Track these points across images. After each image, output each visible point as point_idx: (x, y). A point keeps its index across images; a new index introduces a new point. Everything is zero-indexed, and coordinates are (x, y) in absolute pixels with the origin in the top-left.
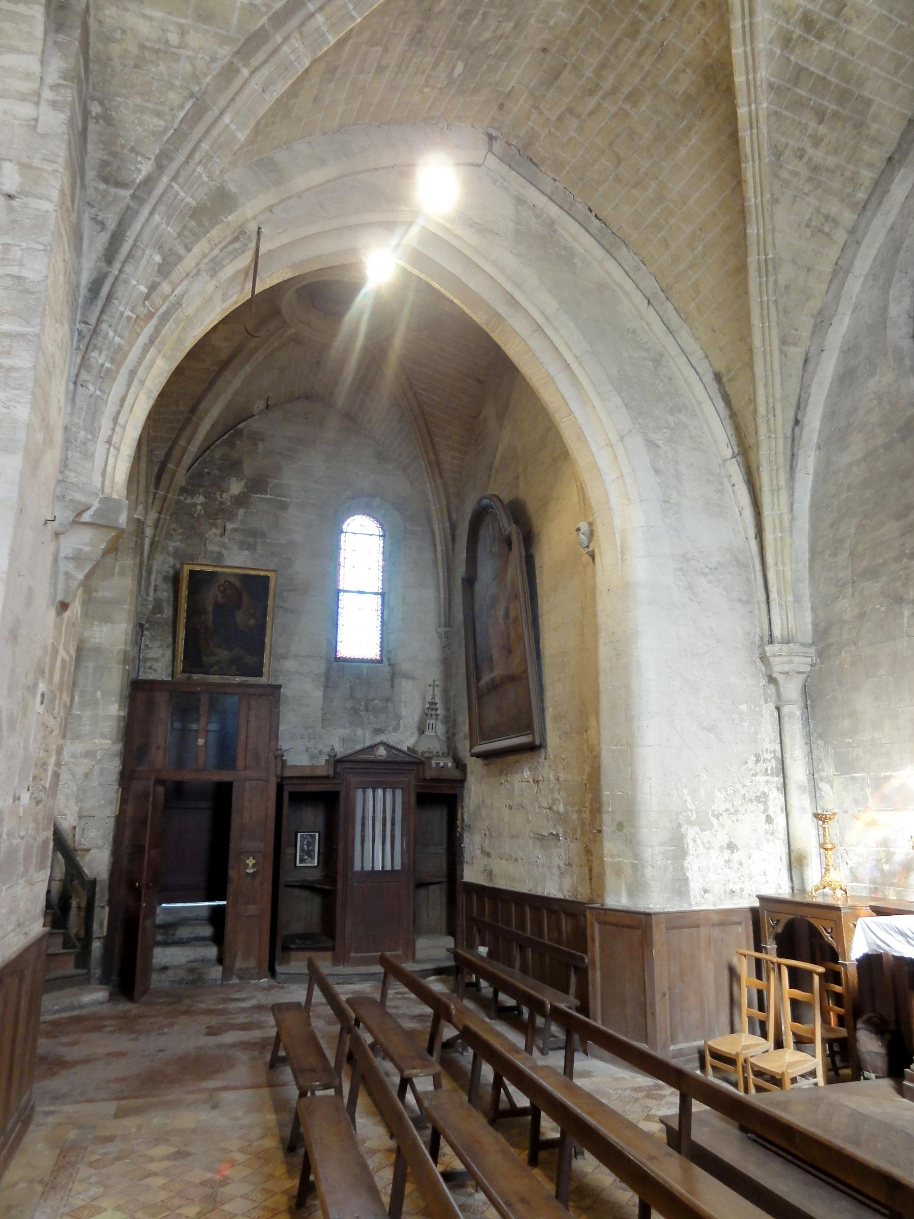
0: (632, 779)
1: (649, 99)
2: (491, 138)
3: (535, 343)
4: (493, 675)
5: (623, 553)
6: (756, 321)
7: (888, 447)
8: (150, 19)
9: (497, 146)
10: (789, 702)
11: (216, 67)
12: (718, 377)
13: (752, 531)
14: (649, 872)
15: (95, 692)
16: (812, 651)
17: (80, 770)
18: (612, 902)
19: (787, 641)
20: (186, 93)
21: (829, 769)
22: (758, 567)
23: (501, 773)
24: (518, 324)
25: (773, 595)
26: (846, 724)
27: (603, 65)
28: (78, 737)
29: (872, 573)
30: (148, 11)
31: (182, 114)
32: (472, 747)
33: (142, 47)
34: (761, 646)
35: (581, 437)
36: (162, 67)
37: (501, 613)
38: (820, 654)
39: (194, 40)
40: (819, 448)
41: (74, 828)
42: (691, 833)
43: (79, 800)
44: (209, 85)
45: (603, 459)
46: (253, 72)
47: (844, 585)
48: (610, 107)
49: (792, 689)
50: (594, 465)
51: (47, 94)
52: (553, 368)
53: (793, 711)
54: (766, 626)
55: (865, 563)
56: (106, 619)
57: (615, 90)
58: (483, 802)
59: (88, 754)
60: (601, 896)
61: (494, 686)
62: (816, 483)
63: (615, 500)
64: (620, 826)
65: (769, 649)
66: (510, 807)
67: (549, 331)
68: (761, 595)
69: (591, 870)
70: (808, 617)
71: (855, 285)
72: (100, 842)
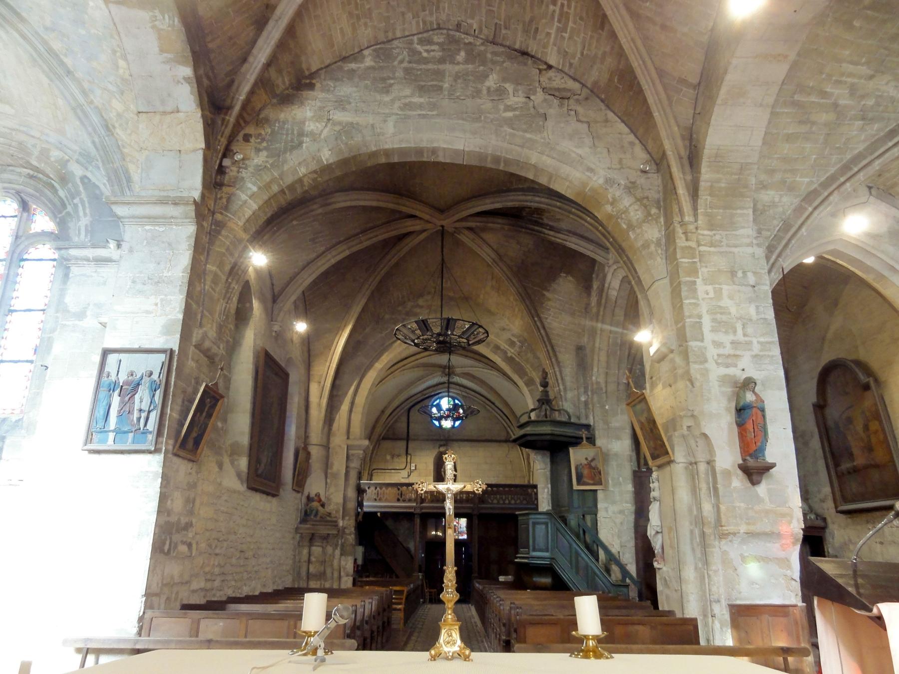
2: (870, 188)
4: (855, 464)
8: (768, 195)
9: (873, 191)
11: (793, 207)
15: (619, 478)
17: (618, 521)
20: (780, 220)
23: (868, 522)
28: (614, 503)
30: (768, 192)
31: (778, 228)
32: (836, 507)
33: (764, 206)
36: (771, 211)
37: (859, 428)
39: (785, 199)
41: (619, 552)
43: (619, 537)
44: (790, 215)
46: (815, 208)
51: (755, 242)
56: (618, 438)
58: (850, 541)
59: (621, 512)
61: (855, 470)
66: (881, 543)
72: (631, 560)
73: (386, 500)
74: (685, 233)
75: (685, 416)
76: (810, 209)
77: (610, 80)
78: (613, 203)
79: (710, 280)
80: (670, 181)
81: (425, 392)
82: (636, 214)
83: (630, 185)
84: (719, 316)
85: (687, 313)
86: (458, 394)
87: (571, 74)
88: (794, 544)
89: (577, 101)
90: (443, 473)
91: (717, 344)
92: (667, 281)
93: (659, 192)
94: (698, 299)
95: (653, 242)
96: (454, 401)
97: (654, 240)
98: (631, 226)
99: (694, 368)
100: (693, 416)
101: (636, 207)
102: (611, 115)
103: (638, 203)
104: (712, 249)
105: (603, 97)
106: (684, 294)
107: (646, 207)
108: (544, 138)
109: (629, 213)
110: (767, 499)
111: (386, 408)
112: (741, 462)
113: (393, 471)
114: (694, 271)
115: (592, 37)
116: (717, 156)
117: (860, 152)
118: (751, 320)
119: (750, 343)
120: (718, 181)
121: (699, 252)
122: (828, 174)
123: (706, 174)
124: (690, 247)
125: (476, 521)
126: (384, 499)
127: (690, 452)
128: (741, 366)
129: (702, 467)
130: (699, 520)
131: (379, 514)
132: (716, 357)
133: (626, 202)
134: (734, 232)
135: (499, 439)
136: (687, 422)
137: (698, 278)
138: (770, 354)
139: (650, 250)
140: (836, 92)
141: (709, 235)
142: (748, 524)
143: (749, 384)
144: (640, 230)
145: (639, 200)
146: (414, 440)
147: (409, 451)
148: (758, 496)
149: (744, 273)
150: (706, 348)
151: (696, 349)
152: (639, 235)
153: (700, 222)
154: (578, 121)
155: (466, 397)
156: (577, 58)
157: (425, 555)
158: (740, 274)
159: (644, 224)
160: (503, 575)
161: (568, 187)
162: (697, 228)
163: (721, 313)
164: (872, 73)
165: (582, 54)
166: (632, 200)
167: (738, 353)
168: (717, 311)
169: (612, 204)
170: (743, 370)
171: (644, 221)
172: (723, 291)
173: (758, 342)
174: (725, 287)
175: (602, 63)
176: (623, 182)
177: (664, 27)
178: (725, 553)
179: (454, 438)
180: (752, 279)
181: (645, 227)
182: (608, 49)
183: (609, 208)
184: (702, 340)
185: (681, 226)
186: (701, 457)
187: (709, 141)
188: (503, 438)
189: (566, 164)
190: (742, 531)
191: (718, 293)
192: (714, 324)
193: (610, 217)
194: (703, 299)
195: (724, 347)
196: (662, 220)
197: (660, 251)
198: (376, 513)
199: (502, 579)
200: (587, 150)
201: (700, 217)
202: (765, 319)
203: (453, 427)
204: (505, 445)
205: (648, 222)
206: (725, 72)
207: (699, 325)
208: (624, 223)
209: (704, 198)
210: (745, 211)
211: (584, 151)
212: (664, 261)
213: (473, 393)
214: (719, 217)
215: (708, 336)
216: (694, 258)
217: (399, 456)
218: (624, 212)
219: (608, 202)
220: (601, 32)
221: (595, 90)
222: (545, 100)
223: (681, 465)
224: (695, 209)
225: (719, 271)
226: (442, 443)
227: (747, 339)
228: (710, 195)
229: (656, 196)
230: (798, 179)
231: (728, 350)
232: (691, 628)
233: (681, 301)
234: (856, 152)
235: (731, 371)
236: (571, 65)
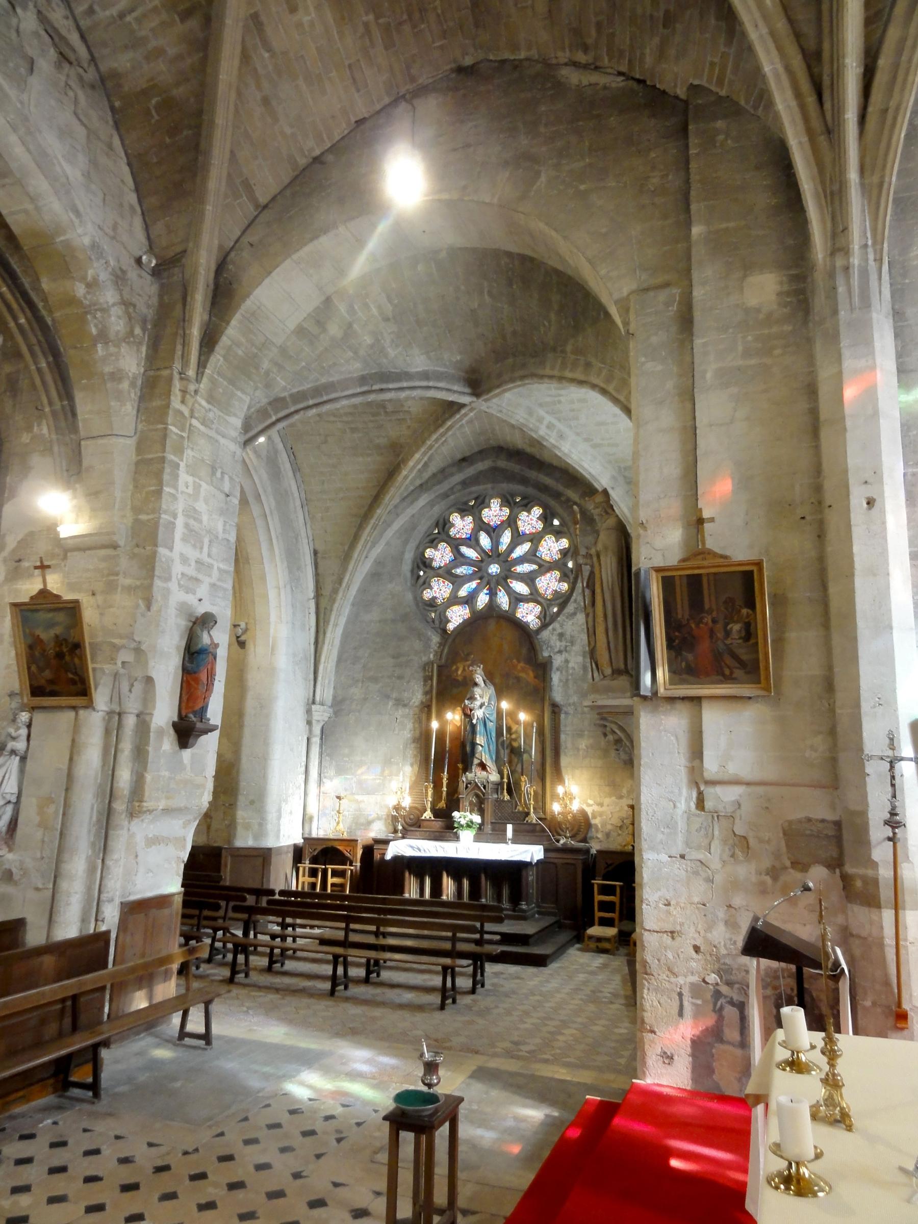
0: (263, 777)
1: (360, 435)
3: (259, 522)
5: (273, 649)
6: (359, 546)
7: (394, 621)
10: (315, 736)
11: (258, 406)
12: (316, 553)
13: (313, 640)
14: (269, 827)
16: (331, 710)
18: (239, 843)
19: (322, 704)
21: (332, 772)
22: (312, 661)
24: (255, 510)
25: (320, 678)
26: (346, 751)
27: (351, 414)
29: (374, 680)
34: (308, 704)
35: (263, 578)
38: (336, 713)
40: (353, 605)
42: (283, 805)
45: (272, 594)
46: (279, 420)
47: (358, 681)
48: (339, 425)
49: (317, 730)
50: (266, 596)
52: (262, 537)
53: (316, 740)
54: (312, 694)
55: (371, 673)
57: (347, 422)
60: (230, 840)
62: (347, 623)
63: (273, 617)
64: (252, 802)
65: (313, 707)
67: (269, 518)
68: (312, 676)
69: (209, 827)
70: (331, 692)
71: (390, 533)
74: (184, 392)
75: (124, 647)
76: (274, 418)
77: (145, 93)
78: (92, 285)
79: (192, 470)
80: (179, 306)
82: (117, 323)
83: (119, 273)
84: (192, 522)
85: (164, 506)
87: (82, 23)
88: (195, 819)
89: (81, 79)
91: (185, 560)
92: (131, 442)
93: (148, 307)
94: (177, 490)
95: (129, 377)
97: (130, 374)
98: (103, 336)
99: (158, 583)
100: (138, 651)
101: (120, 313)
102: (116, 141)
103: (123, 307)
104: (202, 428)
105: (117, 104)
106: (166, 477)
107: (130, 318)
108: (22, 103)
109: (110, 316)
110: (188, 768)
112: (176, 719)
114: (179, 451)
115: (155, 10)
116: (253, 314)
117: (333, 382)
118: (217, 537)
119: (210, 567)
120: (239, 345)
121: (190, 425)
122: (301, 389)
123: (232, 332)
124: (181, 413)
127: (116, 696)
128: (199, 596)
129: (130, 721)
130: (109, 794)
132: (179, 576)
133: (109, 296)
134: (227, 417)
136: (125, 656)
137: (182, 460)
138: (225, 586)
139: (121, 386)
140: (360, 314)
141: (204, 408)
142: (167, 798)
143: (206, 621)
144: (116, 350)
145: (126, 304)
148: (181, 762)
149: (222, 473)
150: (172, 561)
151: (164, 559)
152: (111, 355)
153: (202, 386)
154: (75, 114)
156: (108, 13)
158: (219, 474)
159: (124, 344)
161: (26, 212)
162: (196, 392)
163: (195, 519)
164: (391, 316)
165: (122, 15)
166: (117, 298)
167: (200, 576)
168: (192, 514)
169: (88, 286)
170: (200, 600)
171: (124, 341)
172: (202, 490)
173: (218, 568)
174: (203, 483)
175: (147, 58)
176: (112, 263)
177: (266, 101)
178: (132, 836)
180: (227, 487)
181: (124, 349)
182: (172, 51)
183: (80, 290)
184: (171, 549)
185: (181, 379)
186: (132, 706)
187: (258, 292)
189: (46, 177)
190: (161, 808)
191: (197, 487)
192: (186, 531)
193: (72, 301)
194: (182, 492)
195: (190, 565)
196: (144, 349)
197: (133, 395)
200: (78, 174)
201: (205, 380)
202: (228, 540)
205: (128, 343)
206: (325, 231)
207: (171, 526)
208: (96, 326)
209: (217, 359)
210: (243, 397)
211: (74, 172)
212: (135, 412)
214: (221, 390)
215: (178, 545)
216: (183, 430)
218: (103, 310)
219: (83, 279)
220: (177, 18)
221: (109, 84)
222: (36, 34)
223: (100, 713)
224: (202, 365)
225: (203, 460)
227: (210, 561)
228: (224, 357)
229: (145, 310)
230: (278, 378)
231: (191, 571)
232: (102, 944)
233: (160, 484)
234: (331, 380)
235: (191, 599)
236: (91, 11)
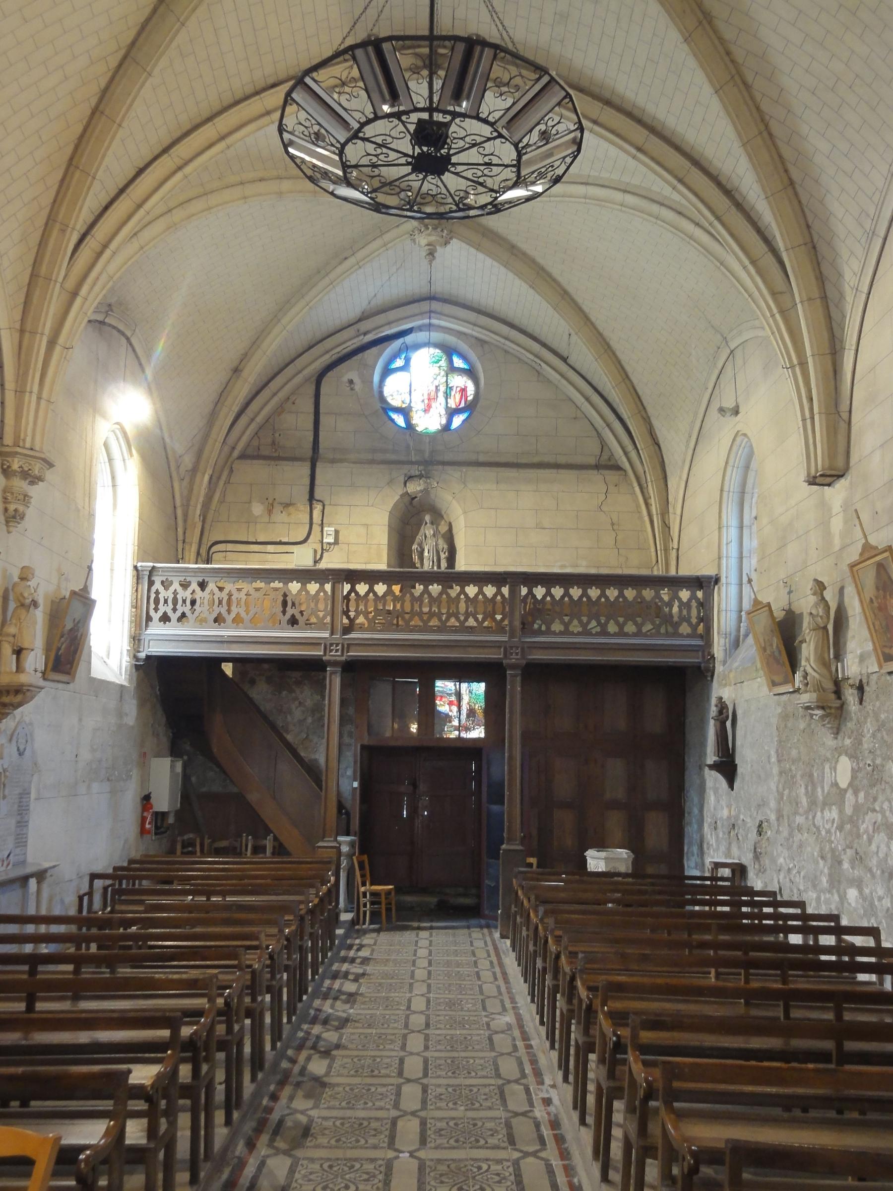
73: (237, 620)
81: (364, 326)
86: (459, 334)
90: (416, 558)
96: (451, 362)
111: (245, 357)
113: (270, 548)
125: (515, 686)
126: (229, 618)
131: (228, 669)
135: (579, 460)
146: (333, 461)
147: (318, 494)
155: (482, 342)
157: (362, 784)
160: (601, 845)
179: (448, 457)
188: (592, 461)
198: (212, 663)
199: (596, 861)
203: (447, 428)
204: (594, 475)
213: (505, 329)
217: (287, 505)
226: (415, 470)
